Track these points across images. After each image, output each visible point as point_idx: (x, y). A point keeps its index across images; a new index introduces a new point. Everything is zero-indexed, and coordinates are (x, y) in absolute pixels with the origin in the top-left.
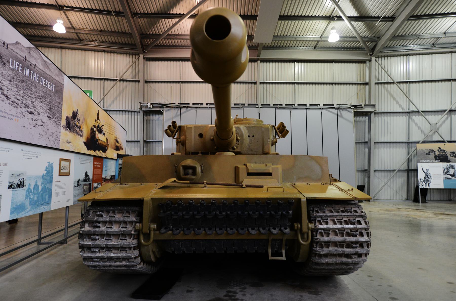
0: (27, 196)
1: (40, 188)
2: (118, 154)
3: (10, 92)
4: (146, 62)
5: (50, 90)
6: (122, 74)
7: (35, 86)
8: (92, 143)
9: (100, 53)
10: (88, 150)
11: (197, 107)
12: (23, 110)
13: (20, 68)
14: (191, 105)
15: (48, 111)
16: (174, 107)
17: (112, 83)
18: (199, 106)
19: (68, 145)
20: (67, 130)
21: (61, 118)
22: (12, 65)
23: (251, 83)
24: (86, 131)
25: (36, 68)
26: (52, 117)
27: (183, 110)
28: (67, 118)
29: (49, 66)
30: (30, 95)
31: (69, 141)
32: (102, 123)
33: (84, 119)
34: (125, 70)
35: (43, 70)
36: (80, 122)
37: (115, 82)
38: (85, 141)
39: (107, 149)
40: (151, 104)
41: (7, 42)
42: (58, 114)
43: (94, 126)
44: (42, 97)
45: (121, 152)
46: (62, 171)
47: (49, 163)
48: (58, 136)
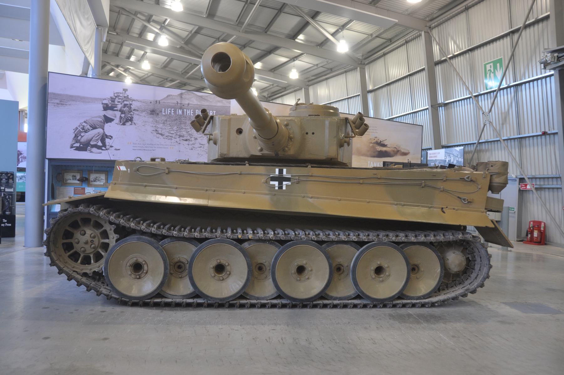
3: (163, 131)
12: (178, 139)
22: (165, 112)
29: (206, 98)
35: (199, 104)
41: (158, 99)
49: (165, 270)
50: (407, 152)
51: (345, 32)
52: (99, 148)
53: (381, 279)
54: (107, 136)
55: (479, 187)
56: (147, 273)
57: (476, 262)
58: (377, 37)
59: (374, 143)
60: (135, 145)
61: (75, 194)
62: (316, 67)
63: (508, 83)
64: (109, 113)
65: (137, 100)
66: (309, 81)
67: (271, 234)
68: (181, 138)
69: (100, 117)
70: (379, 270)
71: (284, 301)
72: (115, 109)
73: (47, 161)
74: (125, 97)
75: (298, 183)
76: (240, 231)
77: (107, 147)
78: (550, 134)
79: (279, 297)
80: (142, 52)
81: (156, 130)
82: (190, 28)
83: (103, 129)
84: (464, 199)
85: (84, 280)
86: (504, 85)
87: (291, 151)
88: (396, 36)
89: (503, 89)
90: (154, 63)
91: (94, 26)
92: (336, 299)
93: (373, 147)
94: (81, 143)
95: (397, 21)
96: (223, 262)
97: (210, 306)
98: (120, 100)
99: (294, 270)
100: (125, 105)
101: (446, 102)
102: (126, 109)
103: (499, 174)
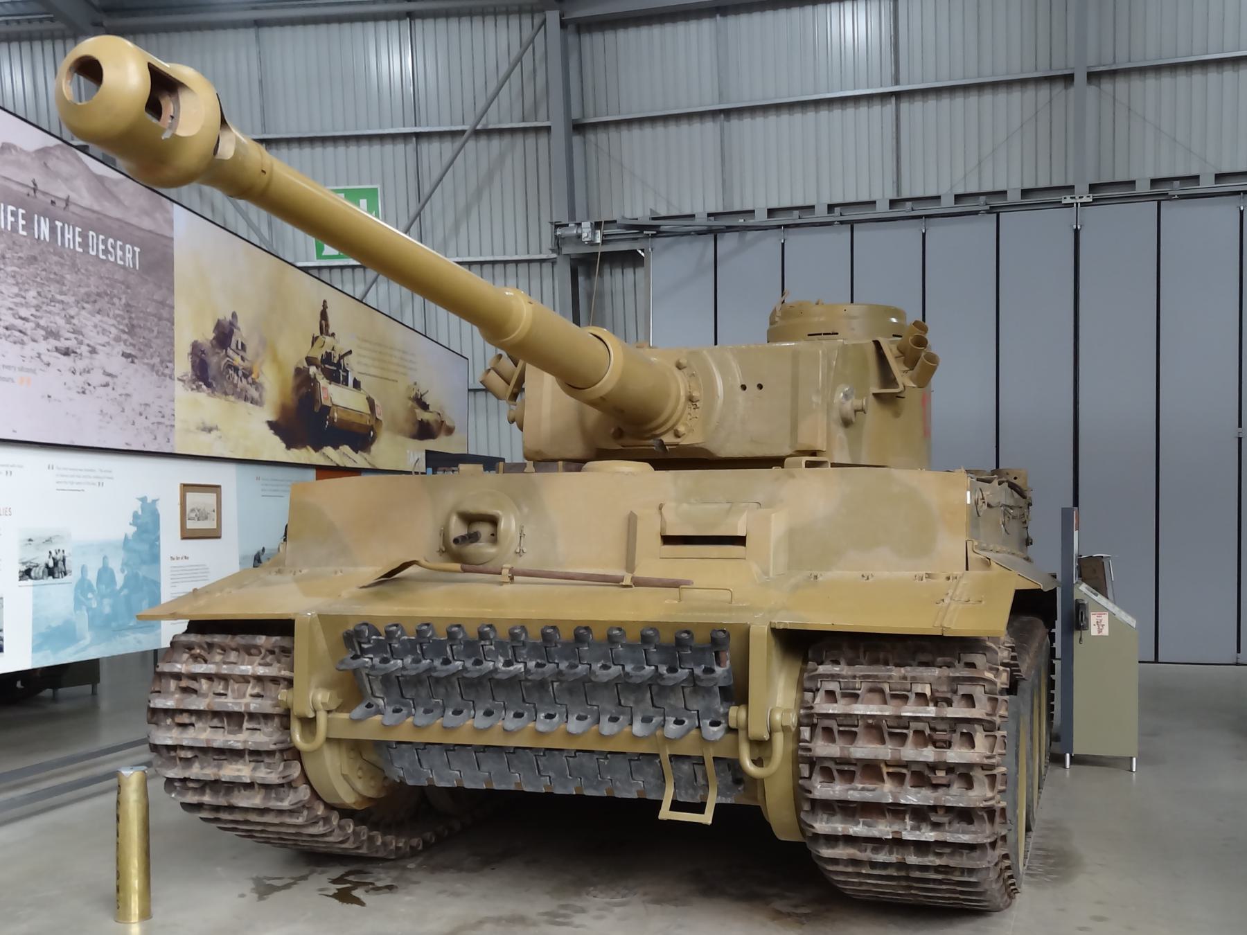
0: (78, 603)
1: (120, 579)
2: (429, 453)
4: (572, 39)
5: (124, 267)
6: (481, 104)
7: (74, 265)
8: (304, 421)
9: (394, 24)
10: (289, 447)
11: (786, 226)
12: (43, 346)
13: (21, 222)
14: (761, 218)
15: (125, 336)
16: (688, 234)
17: (448, 147)
18: (794, 218)
19: (205, 437)
20: (198, 388)
21: (171, 353)
23: (1051, 80)
24: (274, 385)
25: (72, 208)
26: (139, 354)
27: (728, 242)
28: (197, 353)
30: (59, 297)
31: (209, 423)
32: (342, 341)
33: (264, 343)
34: (492, 87)
35: (96, 207)
36: (249, 354)
37: (458, 143)
38: (272, 418)
39: (373, 440)
40: (597, 225)
42: (158, 341)
43: (310, 361)
44: (99, 295)
45: (441, 444)
46: (191, 525)
47: (143, 500)
48: (167, 412)
68: (53, 343)
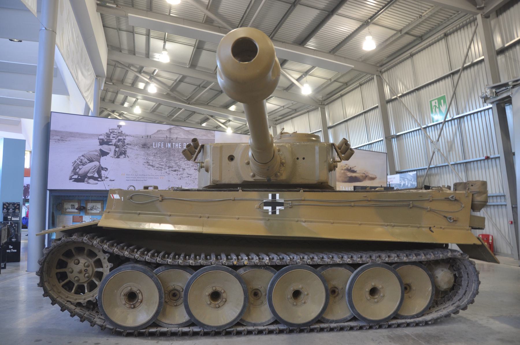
3: (154, 163)
12: (167, 170)
22: (155, 146)
49: (160, 299)
50: (374, 177)
51: (308, 78)
52: (95, 179)
53: (376, 300)
54: (103, 169)
55: (463, 206)
56: (141, 302)
57: (463, 279)
58: (335, 81)
59: (345, 170)
60: (128, 176)
61: (73, 222)
62: (282, 108)
63: (452, 116)
64: (105, 148)
65: (130, 136)
66: (276, 121)
67: (266, 260)
68: (171, 169)
69: (96, 151)
70: (373, 291)
71: (282, 327)
72: (111, 143)
73: (48, 192)
74: (119, 133)
75: (291, 207)
76: (234, 257)
77: (103, 178)
78: (492, 158)
79: (276, 322)
80: (134, 99)
81: (148, 162)
82: (175, 78)
83: (100, 162)
84: (450, 218)
85: (78, 310)
86: (449, 118)
87: (284, 176)
88: (351, 80)
89: (448, 121)
90: (144, 108)
91: (94, 76)
92: (332, 322)
93: (344, 173)
94: (79, 175)
95: (353, 66)
96: (219, 289)
97: (206, 334)
98: (115, 136)
99: (290, 295)
100: (119, 140)
101: (398, 134)
102: (120, 144)
103: (480, 193)
